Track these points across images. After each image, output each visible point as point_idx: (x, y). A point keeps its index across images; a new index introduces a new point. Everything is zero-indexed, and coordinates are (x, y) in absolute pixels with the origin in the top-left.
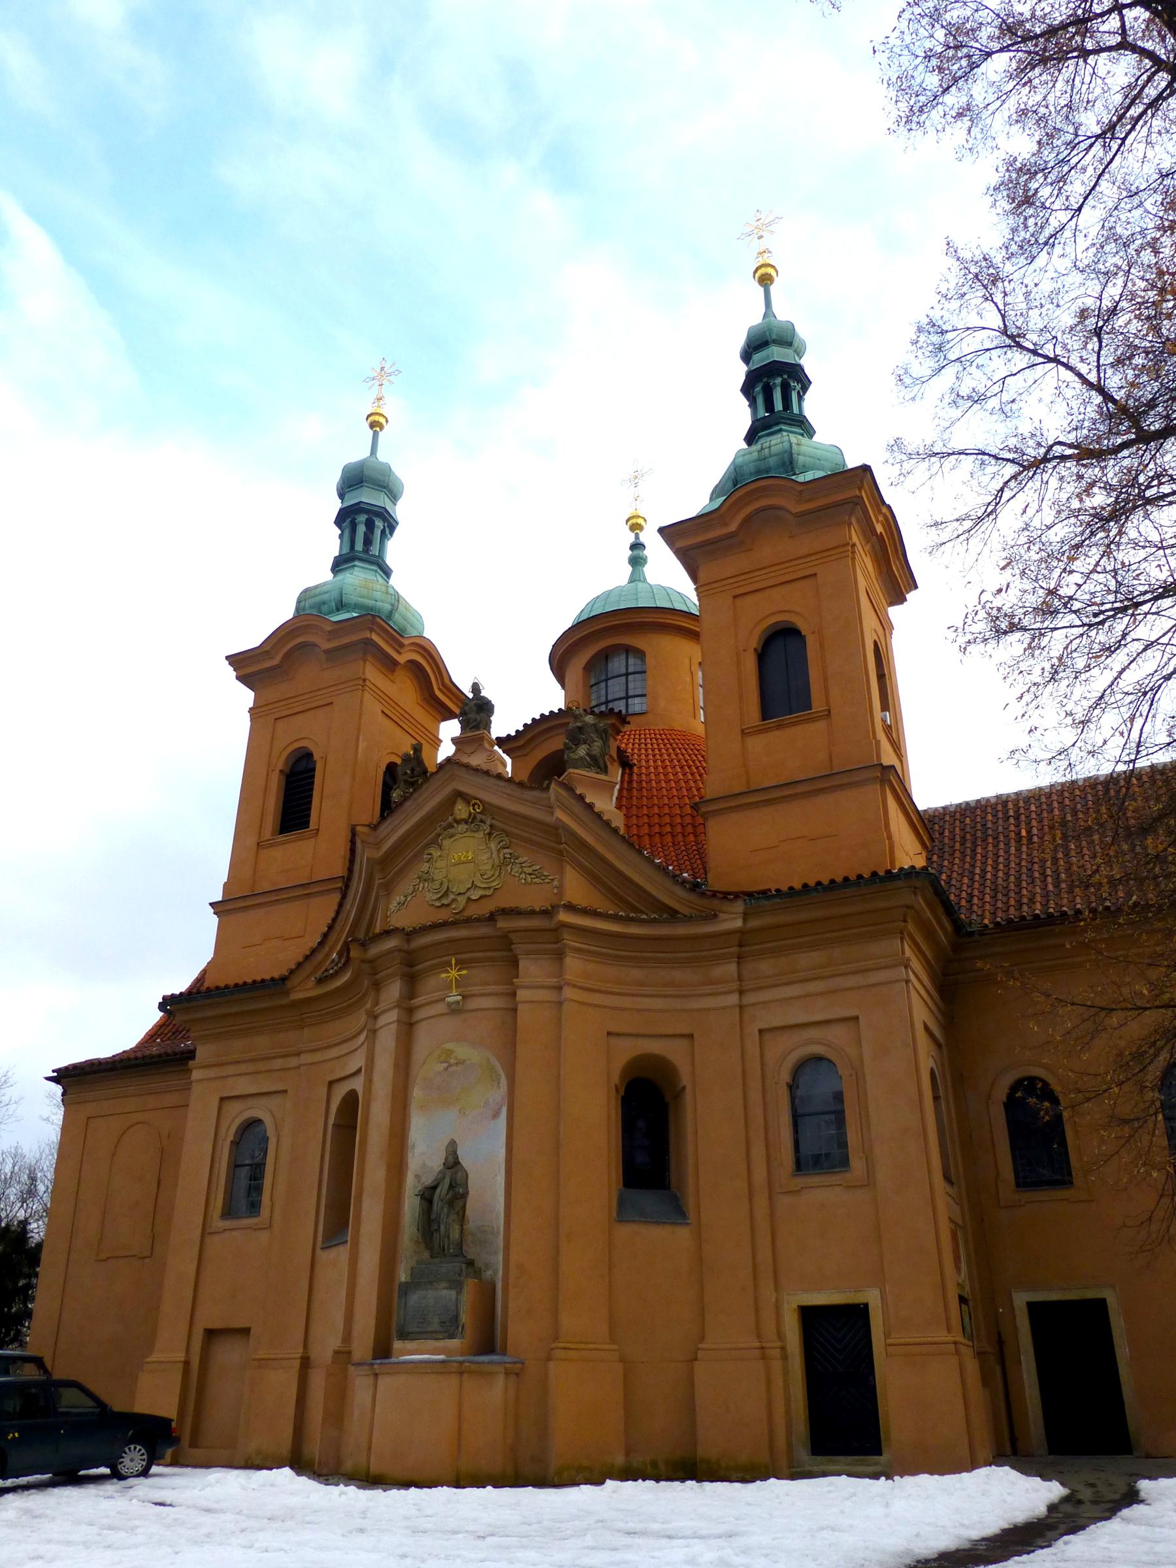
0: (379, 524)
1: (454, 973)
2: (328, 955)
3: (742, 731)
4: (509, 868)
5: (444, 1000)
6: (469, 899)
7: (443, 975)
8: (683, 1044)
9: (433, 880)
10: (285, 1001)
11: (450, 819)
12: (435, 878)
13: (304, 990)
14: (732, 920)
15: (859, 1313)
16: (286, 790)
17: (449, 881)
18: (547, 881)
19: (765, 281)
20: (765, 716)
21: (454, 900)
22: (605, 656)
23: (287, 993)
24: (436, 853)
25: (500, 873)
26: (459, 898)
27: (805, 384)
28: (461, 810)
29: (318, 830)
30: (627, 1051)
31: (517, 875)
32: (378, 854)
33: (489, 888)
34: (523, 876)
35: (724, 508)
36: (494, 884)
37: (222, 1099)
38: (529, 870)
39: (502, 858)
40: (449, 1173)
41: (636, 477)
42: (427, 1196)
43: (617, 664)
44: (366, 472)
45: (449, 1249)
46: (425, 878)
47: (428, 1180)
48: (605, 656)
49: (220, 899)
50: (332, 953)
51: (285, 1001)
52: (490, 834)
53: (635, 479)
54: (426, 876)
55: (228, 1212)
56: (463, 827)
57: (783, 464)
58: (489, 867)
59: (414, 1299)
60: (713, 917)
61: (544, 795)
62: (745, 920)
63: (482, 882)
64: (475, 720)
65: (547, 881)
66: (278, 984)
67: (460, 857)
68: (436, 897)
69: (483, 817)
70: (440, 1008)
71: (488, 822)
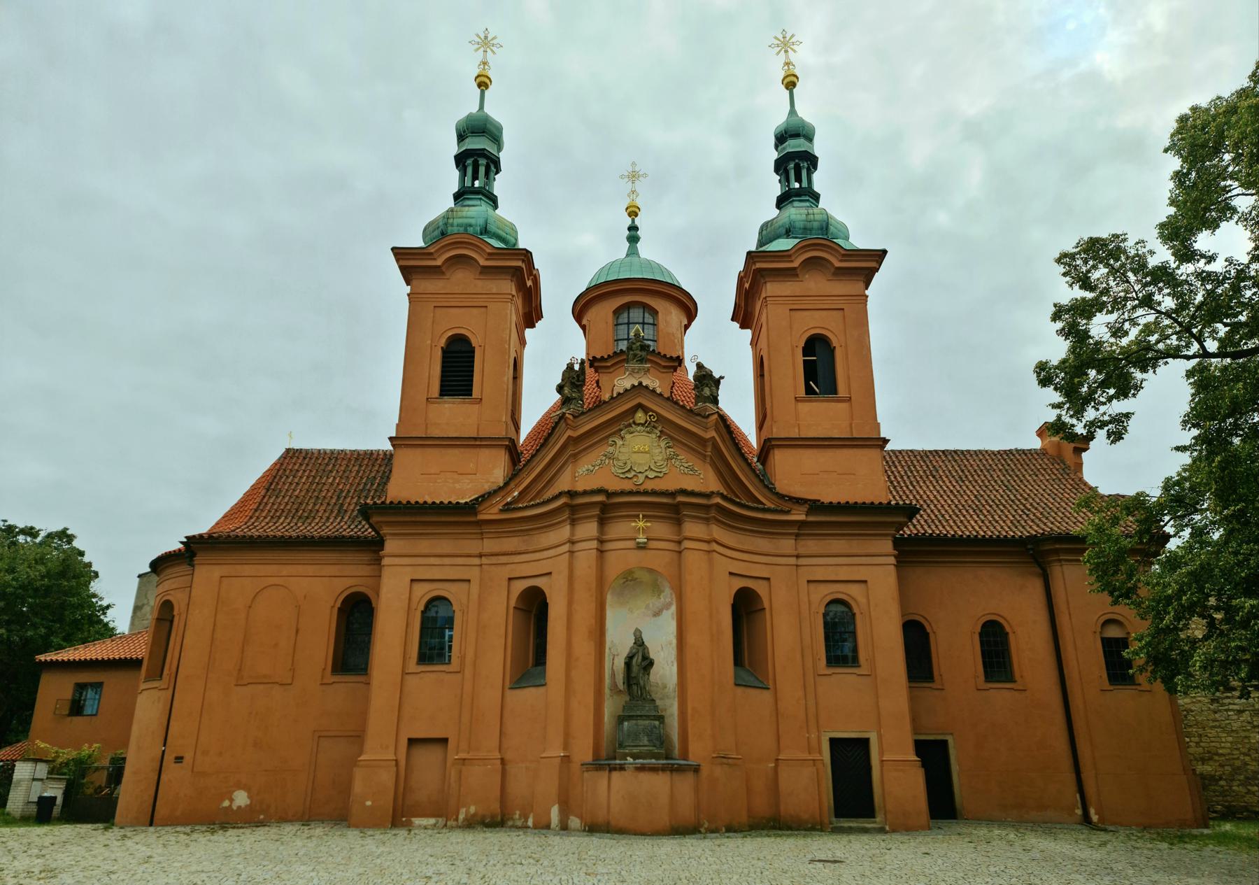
0: (493, 168)
2: (512, 491)
5: (635, 539)
6: (647, 477)
7: (633, 524)
8: (765, 582)
10: (472, 519)
11: (631, 421)
13: (491, 512)
14: (799, 515)
15: (865, 743)
19: (790, 85)
21: (635, 476)
22: (627, 307)
23: (476, 514)
24: (620, 442)
26: (640, 475)
27: (815, 167)
28: (640, 417)
29: (481, 399)
30: (740, 583)
34: (682, 468)
35: (794, 250)
36: (664, 470)
37: (412, 580)
38: (686, 465)
40: (641, 649)
41: (634, 176)
42: (628, 664)
43: (636, 314)
44: (488, 125)
46: (610, 457)
48: (627, 307)
49: (394, 435)
50: (514, 492)
51: (472, 519)
53: (634, 176)
55: (424, 658)
57: (822, 229)
58: (660, 458)
60: (788, 512)
61: (704, 420)
62: (806, 515)
66: (470, 508)
68: (620, 471)
70: (630, 544)
71: (660, 428)
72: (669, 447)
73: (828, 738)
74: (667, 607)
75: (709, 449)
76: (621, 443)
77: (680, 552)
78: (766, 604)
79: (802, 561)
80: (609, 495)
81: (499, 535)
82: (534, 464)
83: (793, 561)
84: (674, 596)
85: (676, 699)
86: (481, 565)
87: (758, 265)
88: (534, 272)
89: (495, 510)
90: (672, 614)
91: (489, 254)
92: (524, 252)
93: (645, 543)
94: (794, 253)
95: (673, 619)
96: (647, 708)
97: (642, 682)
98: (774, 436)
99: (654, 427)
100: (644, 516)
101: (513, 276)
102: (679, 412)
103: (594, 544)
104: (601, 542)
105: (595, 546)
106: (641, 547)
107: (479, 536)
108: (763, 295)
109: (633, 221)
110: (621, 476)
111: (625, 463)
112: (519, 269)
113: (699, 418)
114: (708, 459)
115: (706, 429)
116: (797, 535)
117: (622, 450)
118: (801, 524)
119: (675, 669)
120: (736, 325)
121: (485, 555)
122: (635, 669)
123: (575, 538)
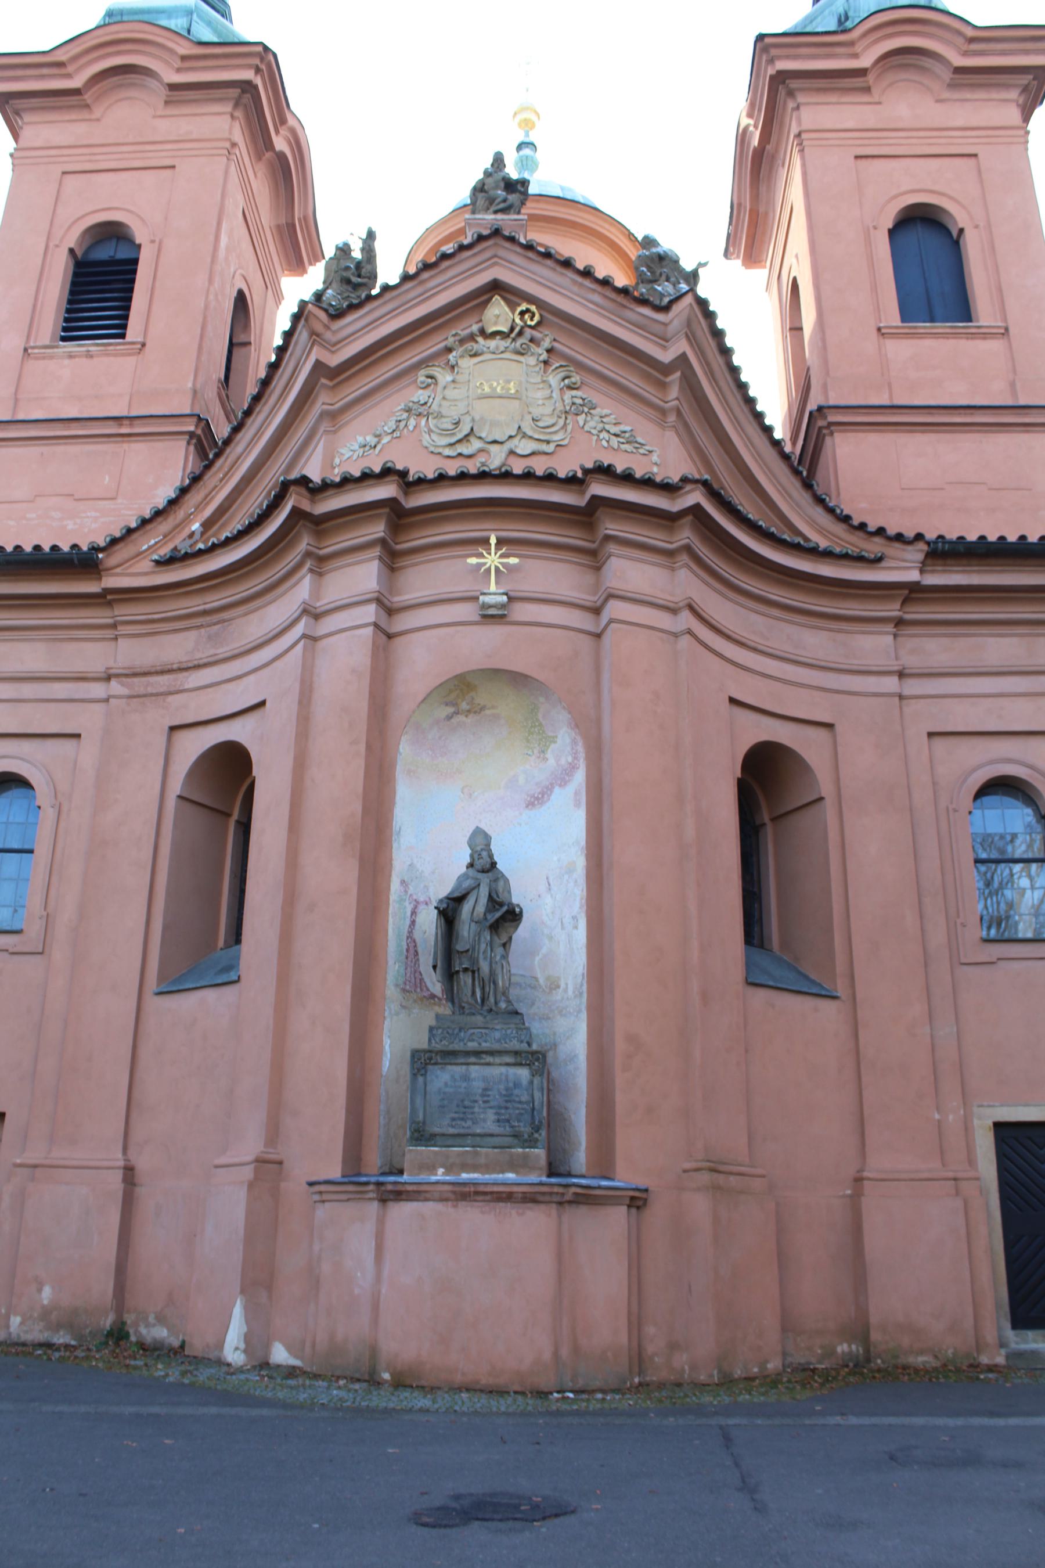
1: (493, 559)
2: (187, 520)
3: (879, 329)
4: (581, 419)
6: (512, 452)
7: (473, 561)
8: (821, 734)
9: (439, 416)
11: (475, 328)
12: (444, 412)
16: (74, 284)
17: (473, 420)
18: (642, 451)
20: (906, 315)
21: (481, 450)
24: (444, 377)
25: (565, 424)
26: (494, 449)
29: (143, 345)
31: (594, 432)
32: (334, 360)
33: (548, 442)
34: (604, 435)
36: (556, 437)
38: (614, 430)
39: (568, 401)
40: (485, 880)
45: (496, 1003)
46: (418, 411)
47: (443, 888)
52: (546, 363)
54: (421, 410)
56: (493, 344)
58: (548, 410)
59: (442, 1078)
61: (660, 317)
62: (922, 571)
63: (535, 431)
64: (505, 201)
65: (642, 451)
67: (494, 389)
69: (536, 334)
71: (547, 344)
72: (570, 388)
73: (990, 1123)
74: (562, 778)
75: (674, 392)
76: (449, 378)
77: (598, 636)
78: (826, 787)
79: (912, 687)
80: (409, 483)
81: (153, 627)
82: (240, 449)
83: (891, 684)
84: (580, 749)
85: (584, 1015)
86: (107, 700)
87: (782, 65)
88: (291, 122)
89: (146, 565)
90: (576, 793)
91: (184, 58)
92: (260, 49)
93: (503, 606)
94: (865, 35)
95: (577, 805)
96: (497, 1035)
97: (484, 967)
98: (832, 403)
99: (532, 340)
100: (500, 542)
101: (236, 105)
102: (596, 298)
103: (369, 613)
104: (391, 611)
105: (372, 619)
106: (492, 617)
107: (109, 633)
108: (794, 130)
109: (527, 135)
110: (447, 452)
111: (457, 423)
112: (247, 87)
113: (646, 311)
114: (672, 418)
115: (664, 340)
116: (899, 622)
117: (450, 393)
118: (913, 592)
119: (581, 935)
120: (737, 264)
121: (117, 676)
122: (466, 929)
123: (322, 604)
